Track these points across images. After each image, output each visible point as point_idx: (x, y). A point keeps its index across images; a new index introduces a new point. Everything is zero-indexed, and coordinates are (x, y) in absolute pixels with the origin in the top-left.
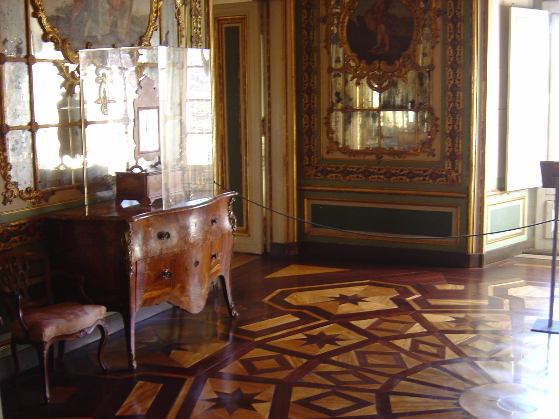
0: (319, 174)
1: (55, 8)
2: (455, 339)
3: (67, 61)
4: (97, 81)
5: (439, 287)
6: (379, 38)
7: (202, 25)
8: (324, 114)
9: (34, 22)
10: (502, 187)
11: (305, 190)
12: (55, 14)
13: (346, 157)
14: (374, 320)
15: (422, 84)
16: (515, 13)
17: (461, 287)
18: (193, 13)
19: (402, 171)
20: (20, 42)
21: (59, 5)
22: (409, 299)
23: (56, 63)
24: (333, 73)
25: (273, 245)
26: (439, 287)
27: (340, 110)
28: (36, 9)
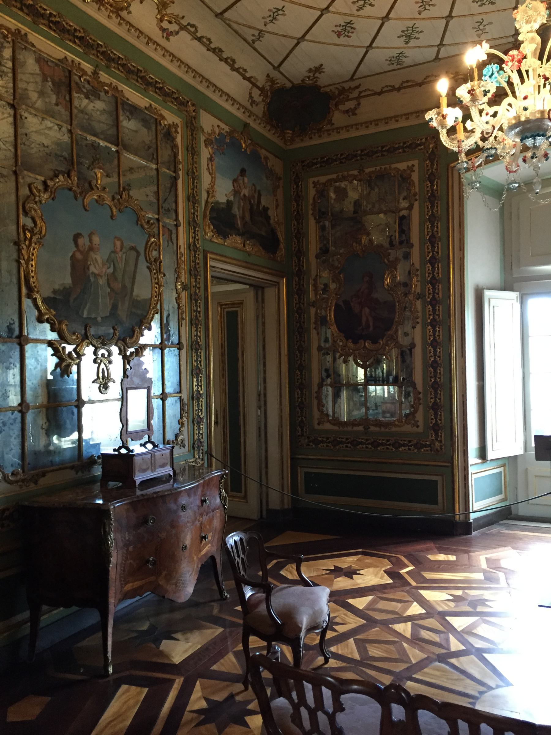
0: (311, 444)
1: (52, 290)
2: (459, 623)
3: (63, 341)
4: (95, 361)
5: (431, 557)
6: (364, 319)
7: (201, 309)
8: (315, 388)
9: (27, 303)
10: (482, 454)
11: (299, 459)
12: (52, 295)
13: (336, 428)
14: (370, 598)
15: (404, 361)
16: (488, 293)
17: (452, 558)
18: (193, 297)
19: (388, 441)
20: (12, 322)
21: (57, 287)
22: (403, 571)
23: (50, 344)
24: (322, 352)
25: (269, 511)
26: (431, 557)
27: (329, 385)
28: (30, 290)
